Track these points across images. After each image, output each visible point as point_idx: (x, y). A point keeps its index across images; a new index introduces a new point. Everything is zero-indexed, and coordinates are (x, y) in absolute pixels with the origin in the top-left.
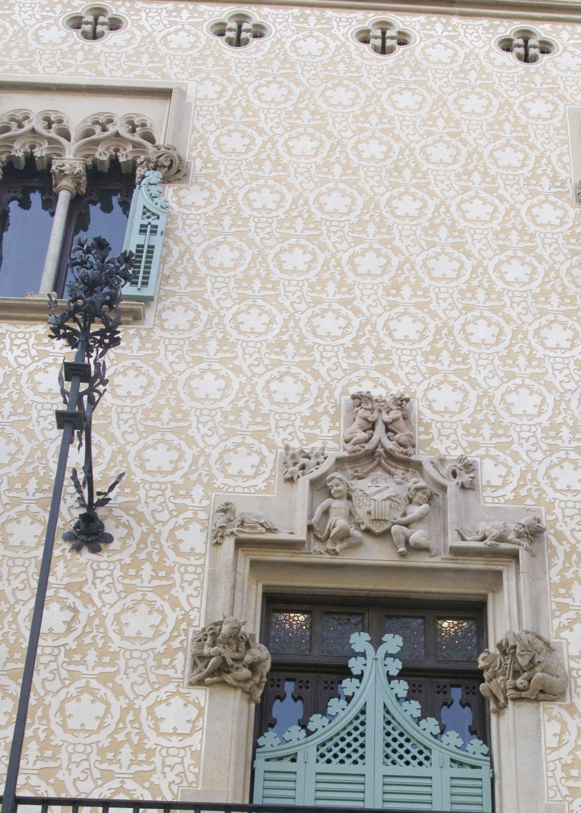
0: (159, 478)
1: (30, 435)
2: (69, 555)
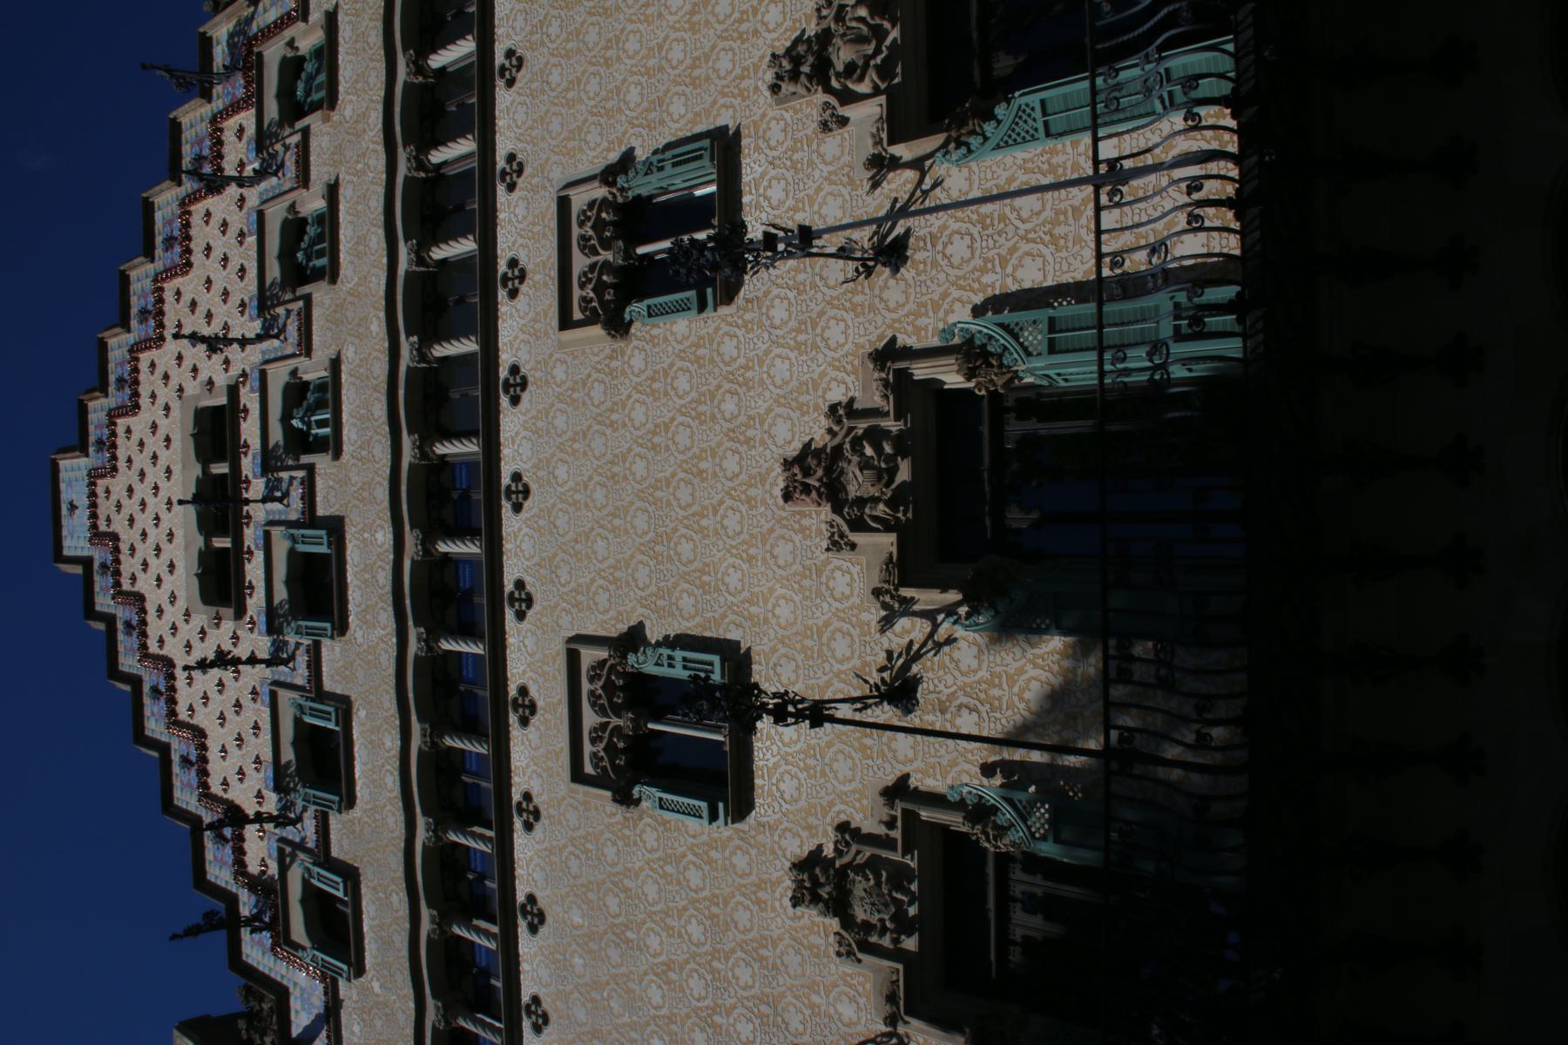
0: (856, 646)
2: (919, 712)
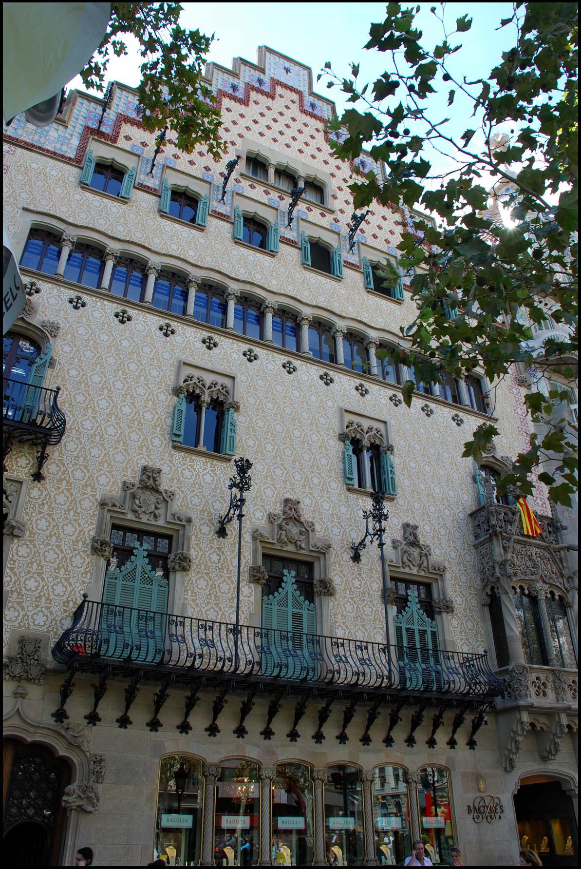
1: (204, 497)
